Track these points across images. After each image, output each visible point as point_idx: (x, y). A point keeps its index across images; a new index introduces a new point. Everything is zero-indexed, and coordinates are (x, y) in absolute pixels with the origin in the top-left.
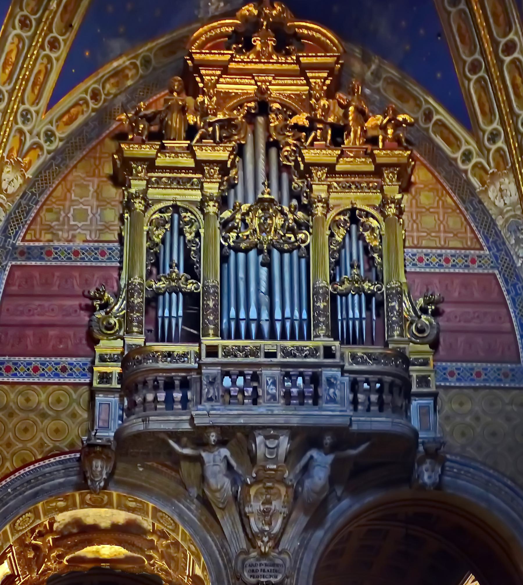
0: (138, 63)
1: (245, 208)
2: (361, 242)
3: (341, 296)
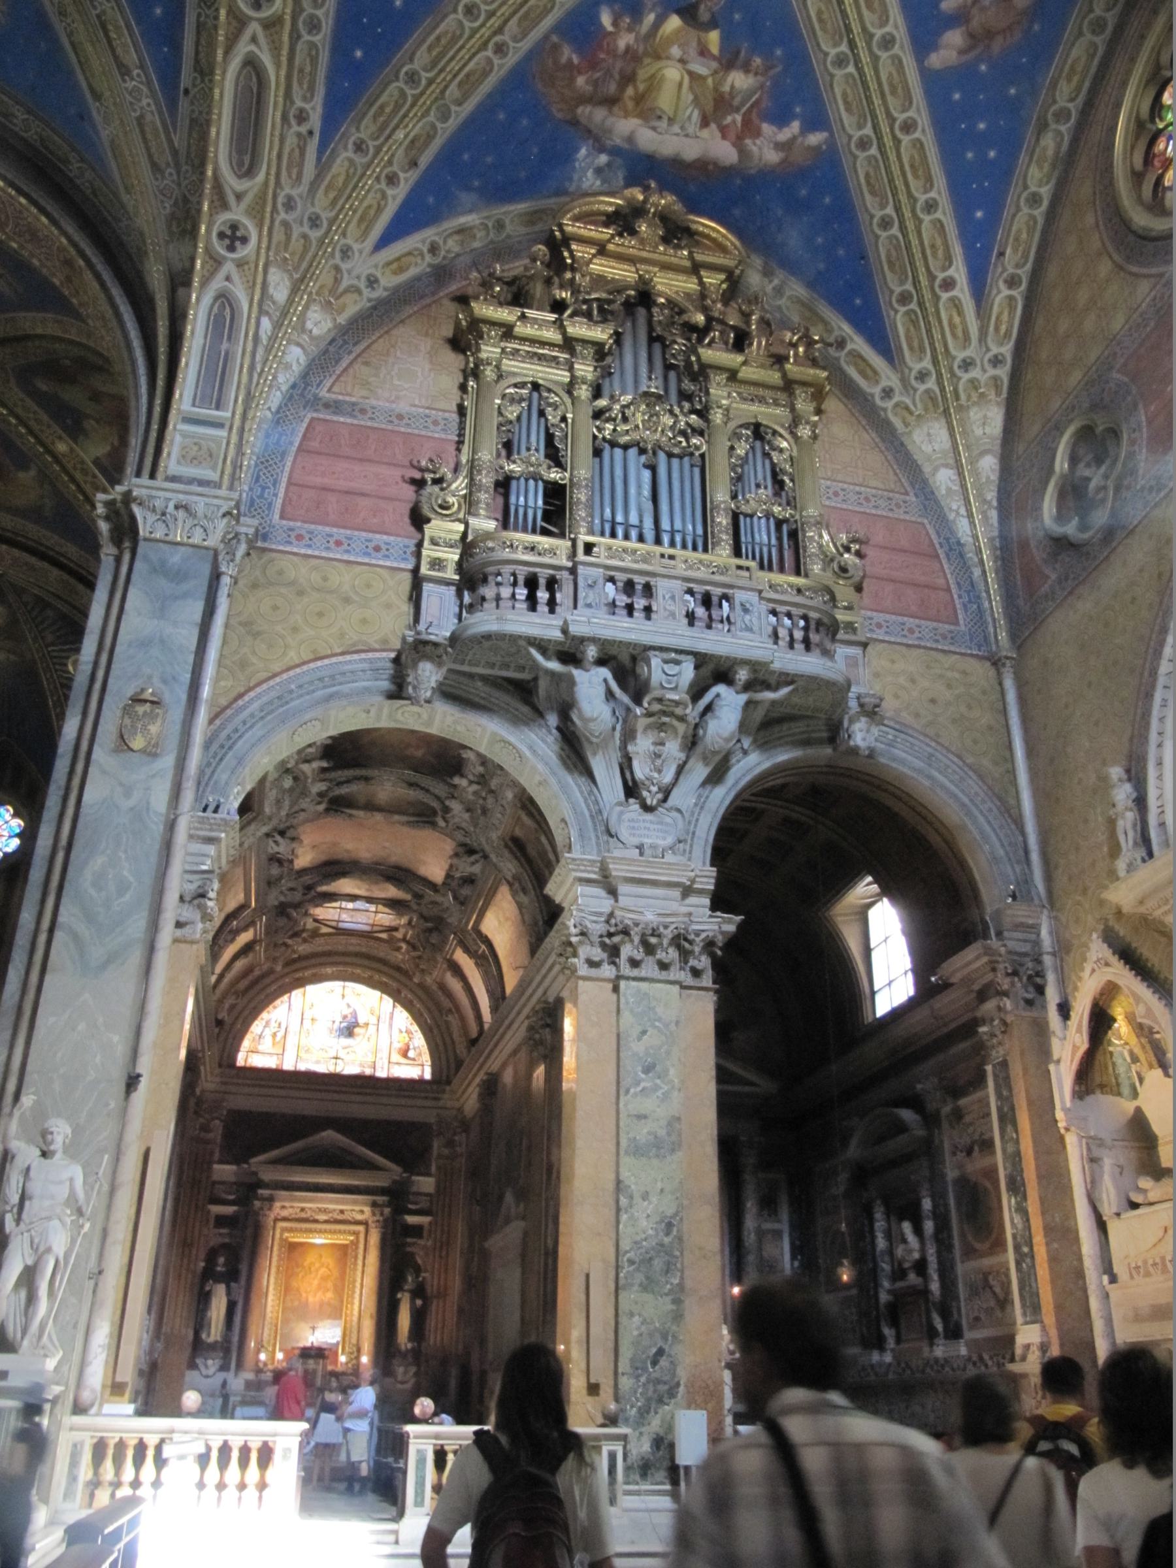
0: (490, 225)
1: (626, 399)
2: (767, 462)
3: (746, 515)
